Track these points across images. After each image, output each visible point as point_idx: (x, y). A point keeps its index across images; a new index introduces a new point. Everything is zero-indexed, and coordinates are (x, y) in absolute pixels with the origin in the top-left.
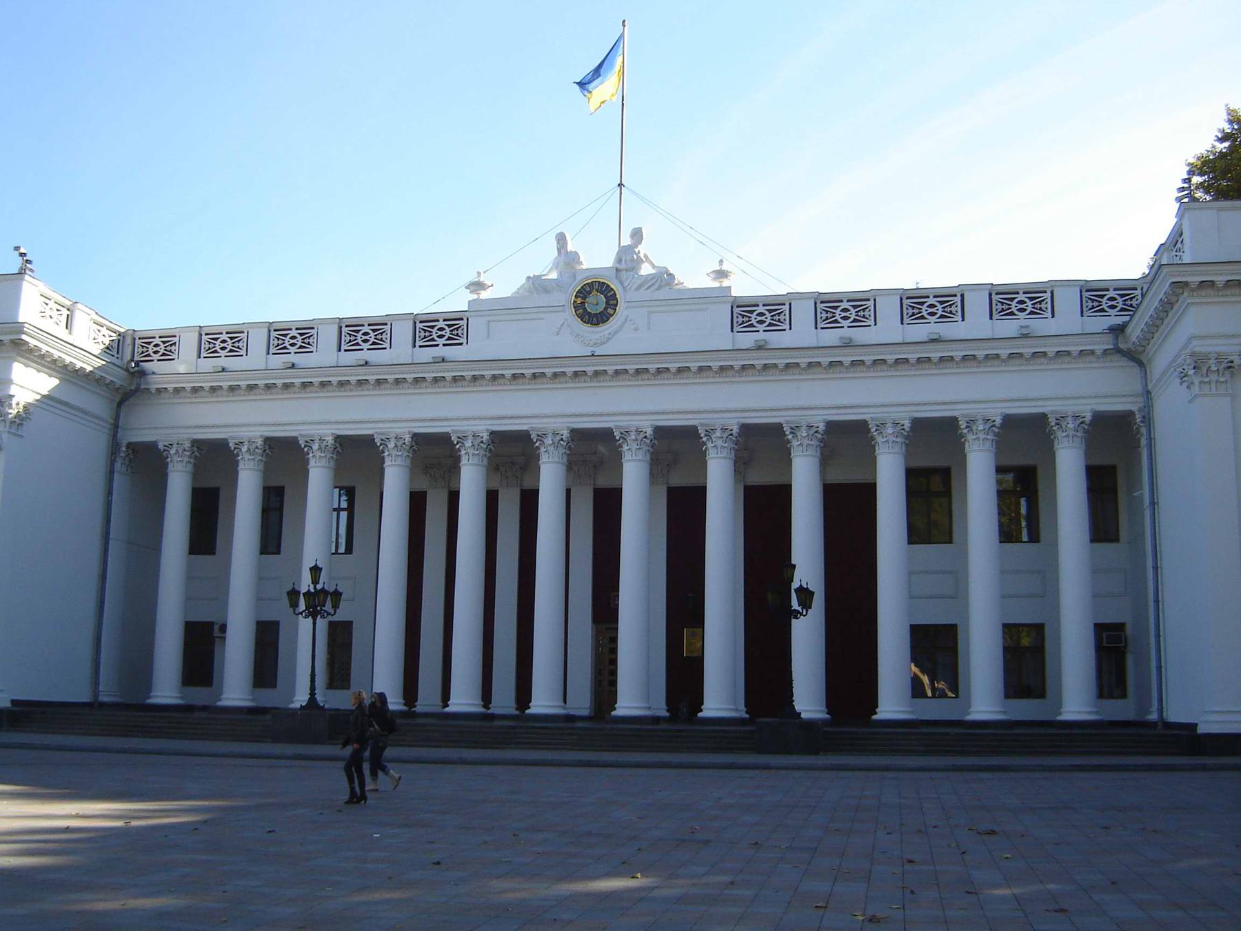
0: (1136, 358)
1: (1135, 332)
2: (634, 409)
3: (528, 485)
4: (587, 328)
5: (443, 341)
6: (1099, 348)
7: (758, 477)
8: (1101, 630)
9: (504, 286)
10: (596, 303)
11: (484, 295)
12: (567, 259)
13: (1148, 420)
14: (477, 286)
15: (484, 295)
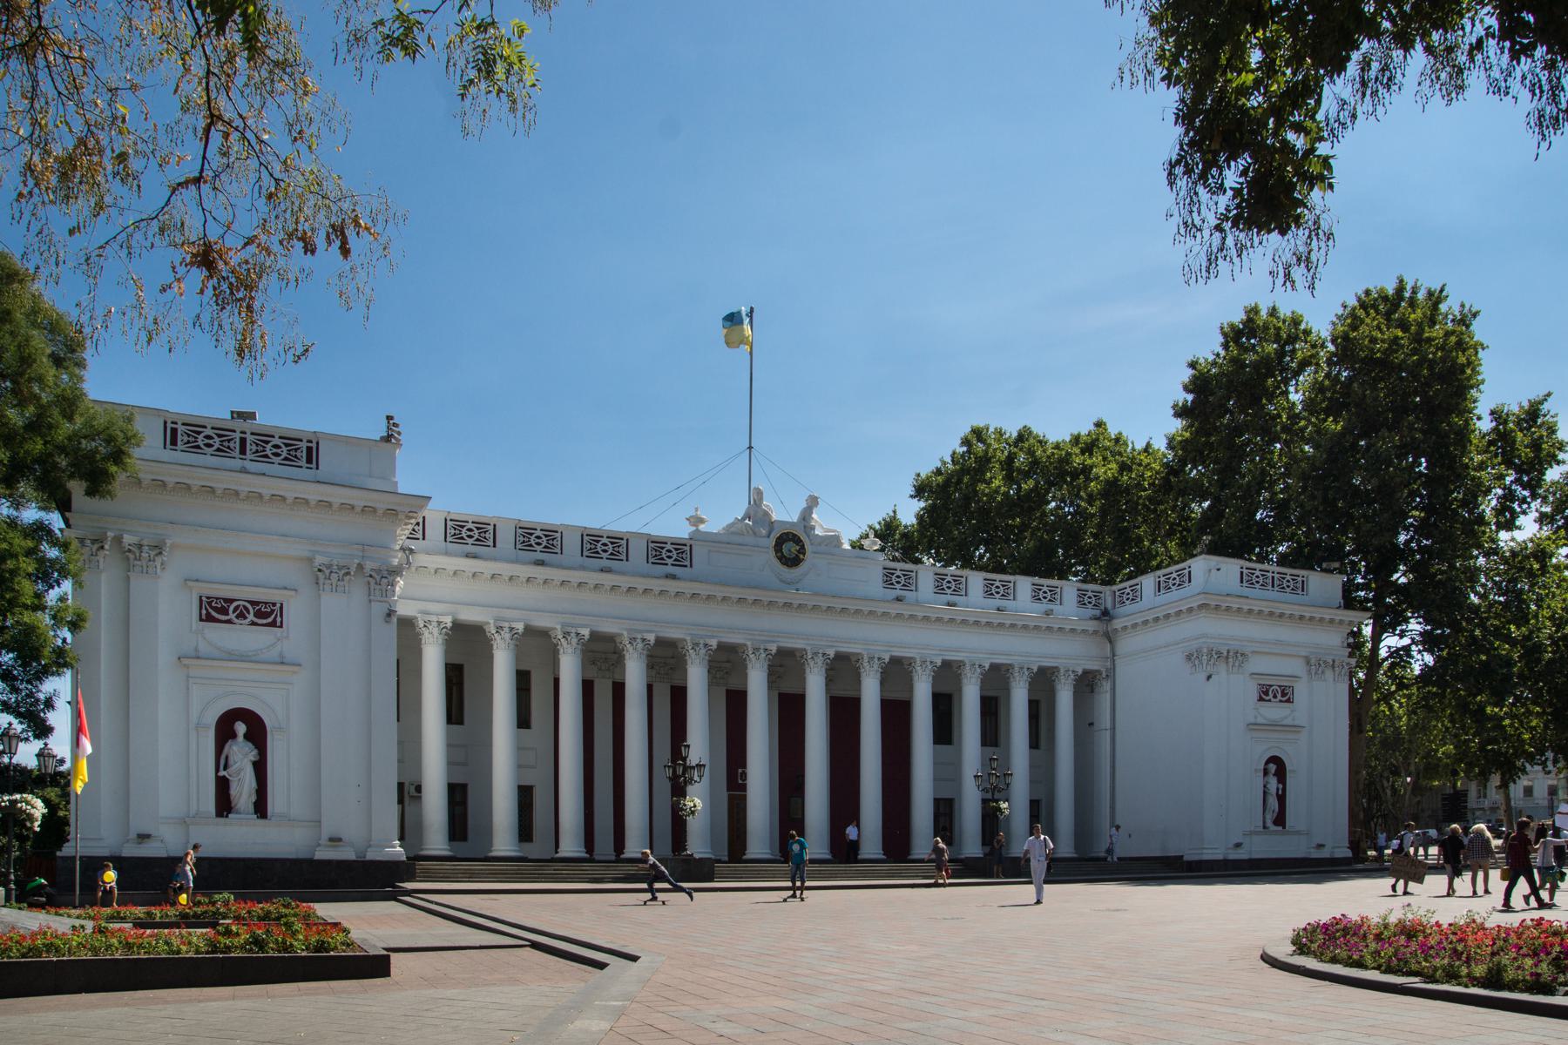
0: (1110, 637)
1: (1117, 624)
2: (818, 635)
3: (618, 678)
4: (784, 569)
5: (670, 561)
6: (1091, 629)
7: (840, 692)
8: (938, 802)
9: (715, 524)
10: (790, 549)
11: (702, 527)
12: (756, 512)
13: (1111, 674)
14: (696, 520)
15: (702, 527)
